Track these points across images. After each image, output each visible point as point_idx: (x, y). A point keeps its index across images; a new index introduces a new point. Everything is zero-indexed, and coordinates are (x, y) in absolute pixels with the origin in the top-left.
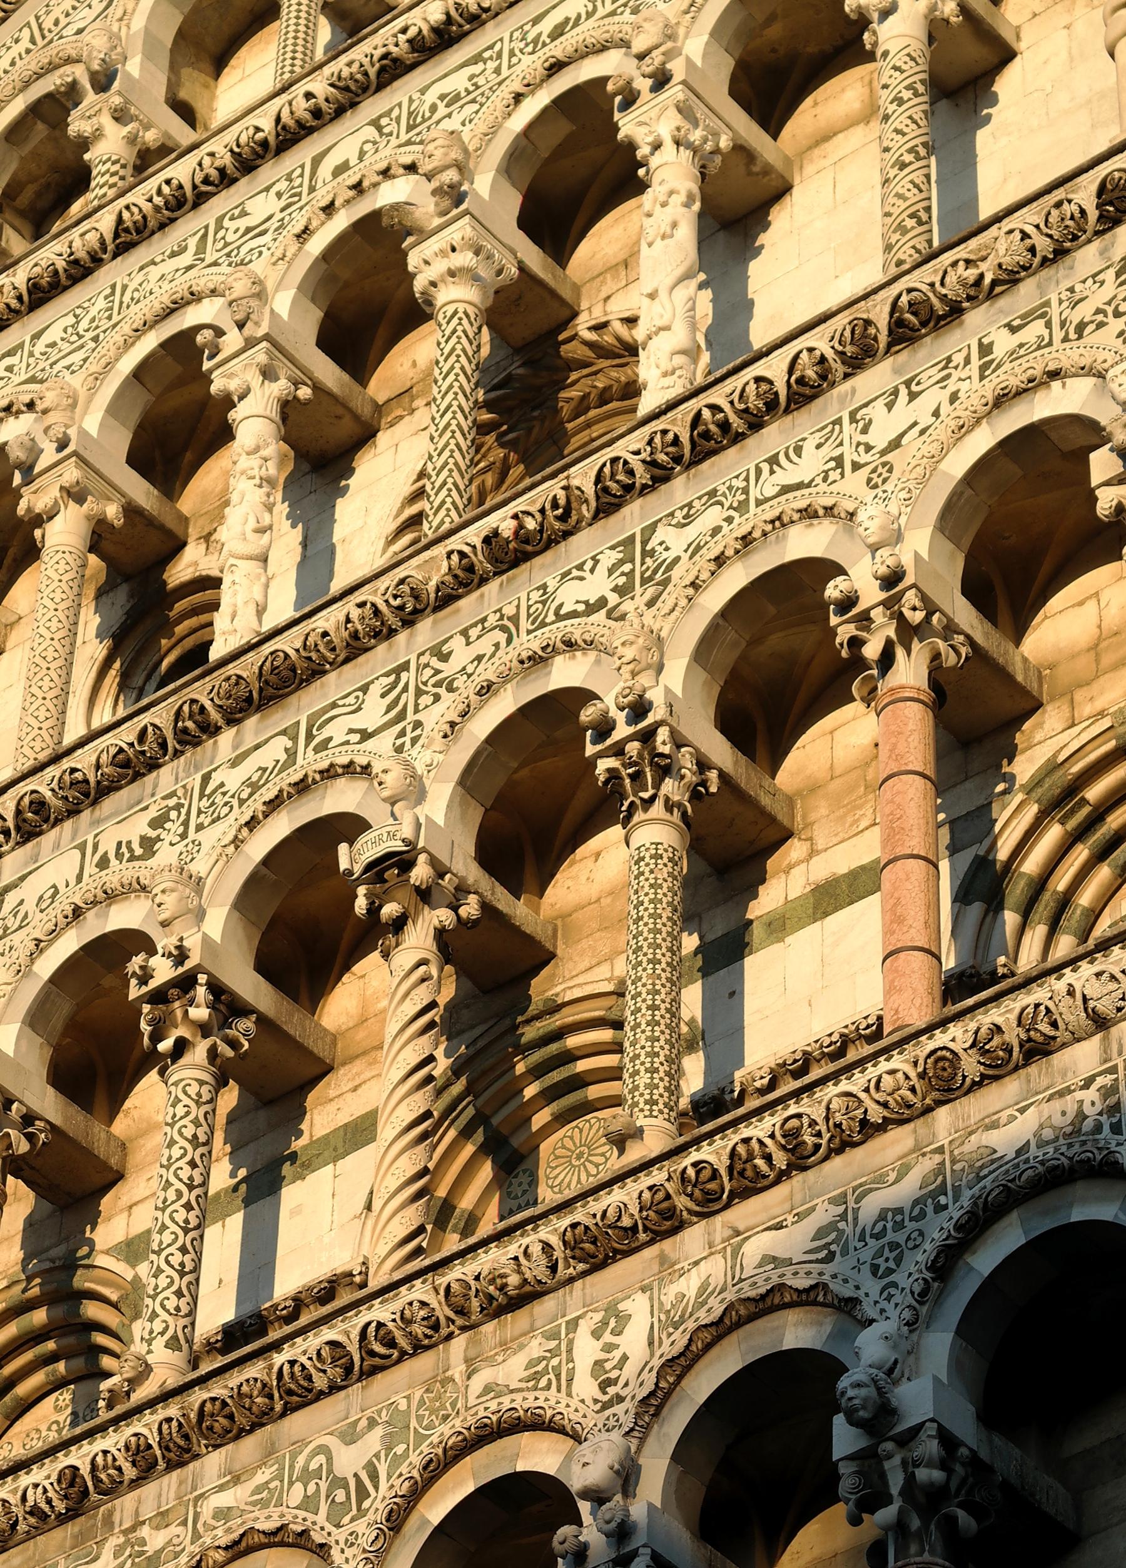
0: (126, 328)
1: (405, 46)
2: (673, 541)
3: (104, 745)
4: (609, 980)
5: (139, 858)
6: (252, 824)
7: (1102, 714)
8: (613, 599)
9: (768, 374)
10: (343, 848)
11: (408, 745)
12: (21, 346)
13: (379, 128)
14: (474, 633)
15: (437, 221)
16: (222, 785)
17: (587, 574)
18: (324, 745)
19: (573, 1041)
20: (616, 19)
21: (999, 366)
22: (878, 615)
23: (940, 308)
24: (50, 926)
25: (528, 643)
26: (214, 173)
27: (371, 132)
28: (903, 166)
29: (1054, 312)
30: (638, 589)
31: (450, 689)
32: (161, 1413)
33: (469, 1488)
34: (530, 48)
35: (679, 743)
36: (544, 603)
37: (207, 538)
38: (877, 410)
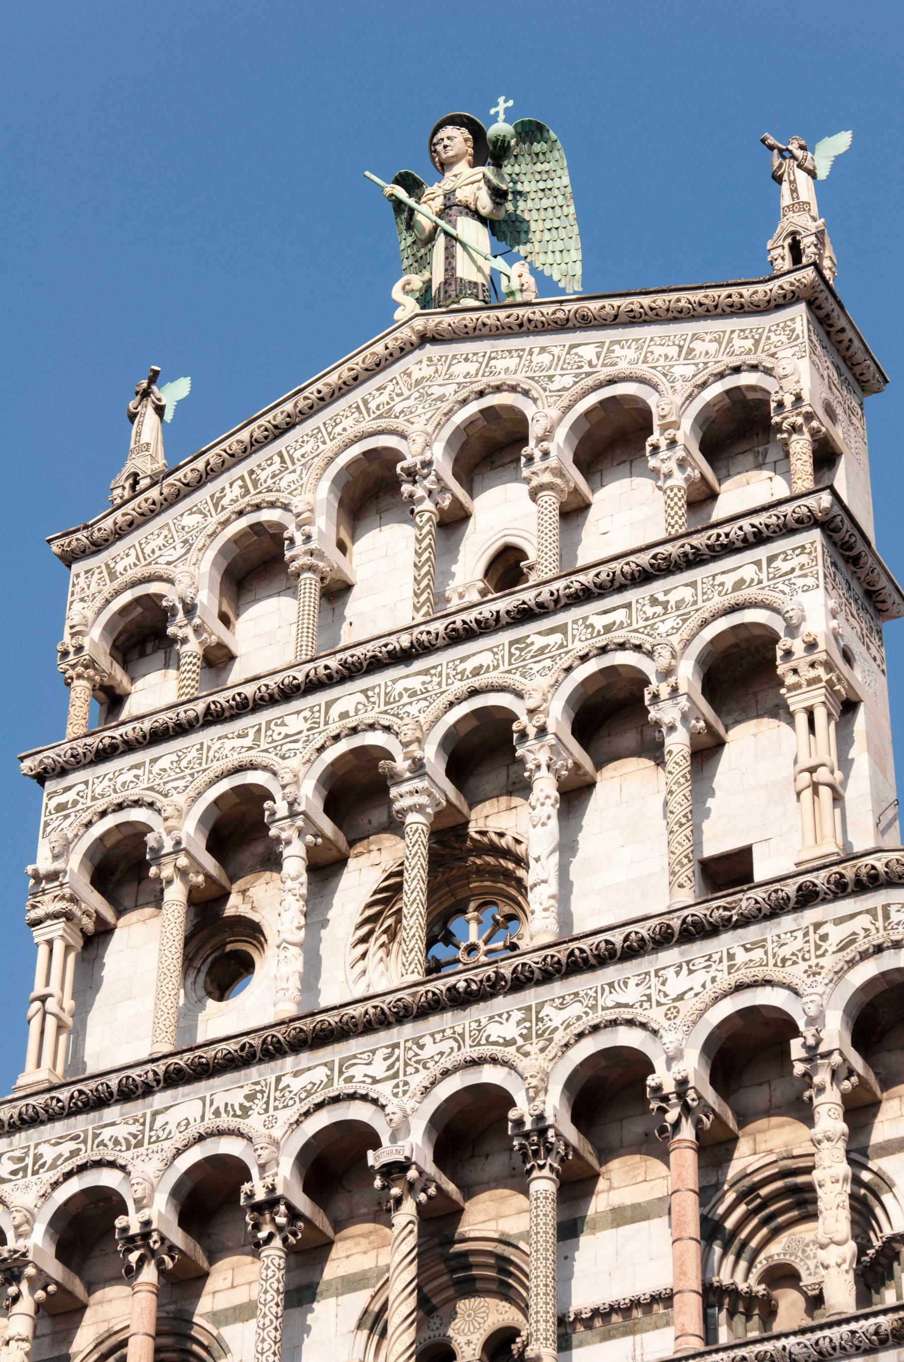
0: (211, 774)
1: (386, 656)
2: (555, 1017)
5: (239, 1116)
6: (307, 1114)
7: (771, 1151)
8: (520, 1041)
9: (613, 939)
10: (370, 1153)
11: (401, 1094)
12: (143, 764)
13: (367, 697)
14: (438, 1037)
15: (408, 775)
16: (288, 1086)
17: (504, 1021)
18: (350, 1079)
20: (512, 676)
21: (738, 969)
22: (673, 1099)
23: (708, 927)
24: (185, 1142)
25: (469, 1052)
27: (361, 698)
28: (681, 825)
29: (769, 946)
30: (534, 1040)
31: (425, 1068)
34: (459, 677)
35: (558, 1135)
36: (479, 1031)
37: (244, 892)
38: (670, 973)
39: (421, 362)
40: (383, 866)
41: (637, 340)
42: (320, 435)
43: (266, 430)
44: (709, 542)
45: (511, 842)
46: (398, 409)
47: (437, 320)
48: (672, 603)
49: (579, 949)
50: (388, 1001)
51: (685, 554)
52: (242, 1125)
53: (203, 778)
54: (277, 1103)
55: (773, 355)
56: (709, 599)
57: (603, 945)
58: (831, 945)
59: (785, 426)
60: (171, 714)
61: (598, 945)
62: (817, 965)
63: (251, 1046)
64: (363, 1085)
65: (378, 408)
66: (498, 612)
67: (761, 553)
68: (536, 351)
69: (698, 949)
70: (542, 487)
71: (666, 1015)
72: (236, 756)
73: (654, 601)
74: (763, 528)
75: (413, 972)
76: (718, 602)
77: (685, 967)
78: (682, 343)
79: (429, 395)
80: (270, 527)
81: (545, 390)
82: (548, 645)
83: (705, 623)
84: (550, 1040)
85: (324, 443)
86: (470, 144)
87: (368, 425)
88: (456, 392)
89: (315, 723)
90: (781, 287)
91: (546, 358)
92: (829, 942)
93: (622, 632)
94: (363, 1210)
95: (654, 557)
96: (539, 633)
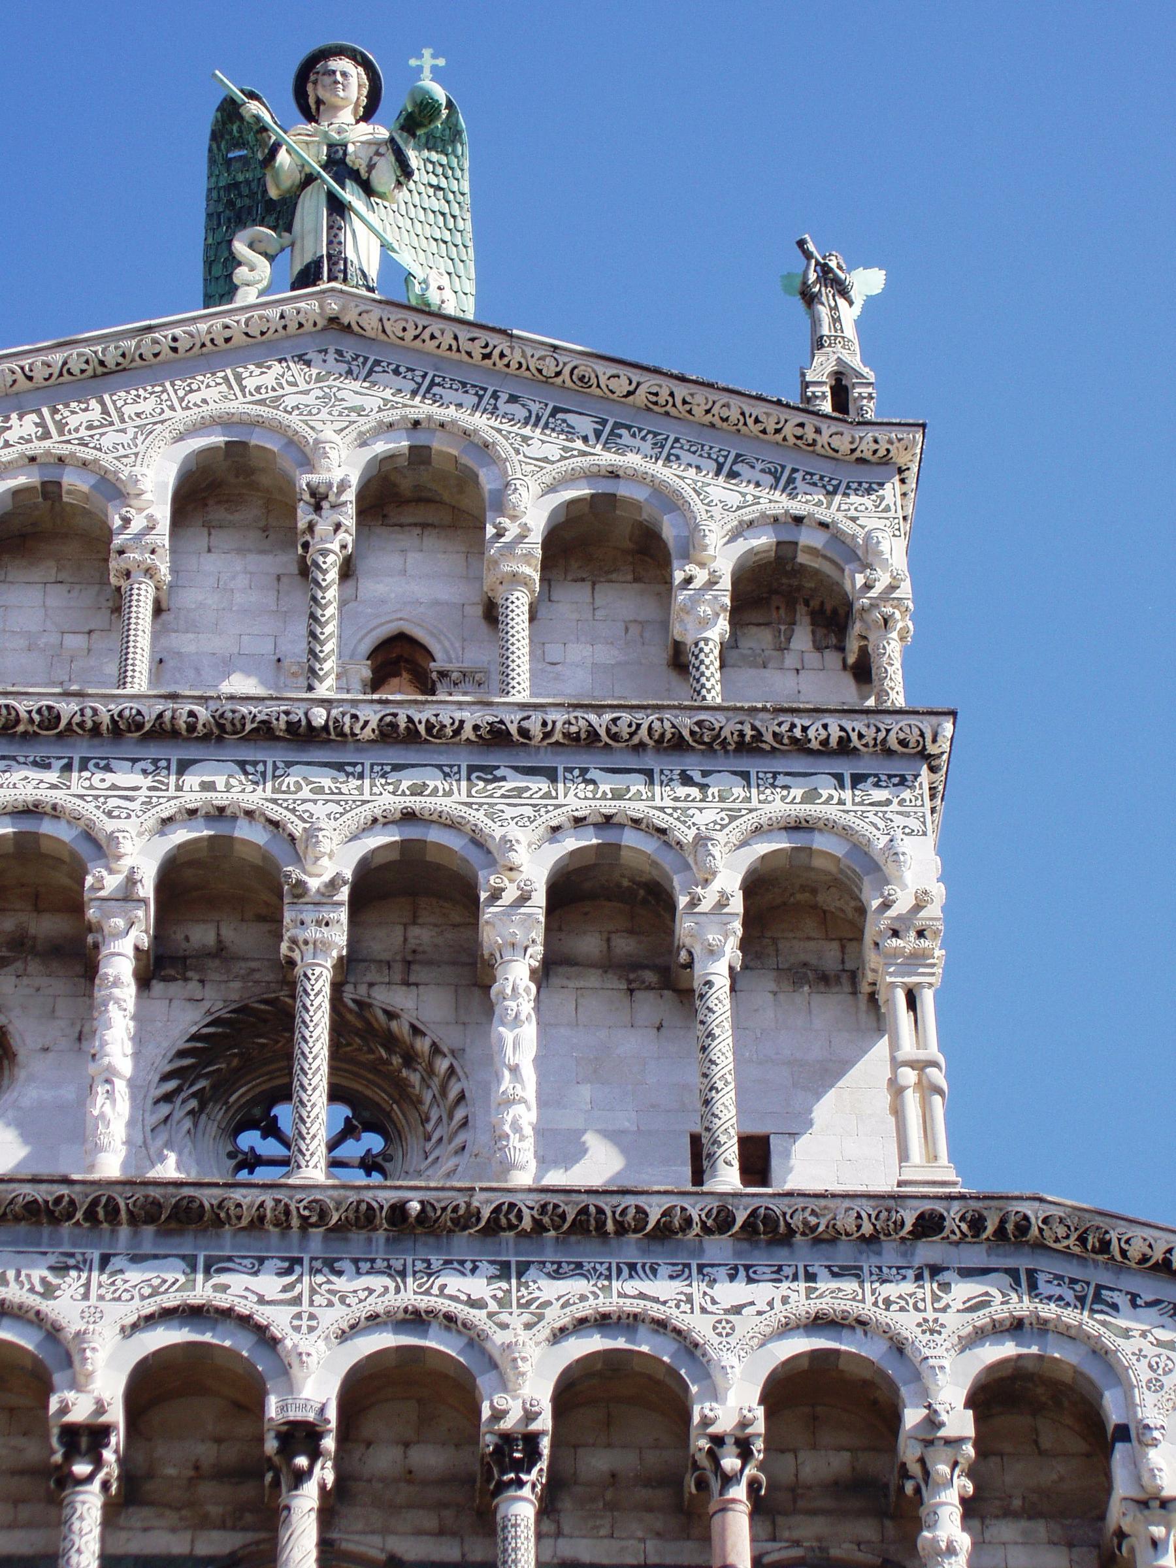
1: (283, 726)
3: (27, 1191)
4: (382, 1550)
7: (797, 1543)
8: (493, 1306)
11: (304, 1329)
17: (468, 1272)
20: (474, 813)
21: (820, 1296)
26: (89, 724)
31: (342, 1300)
39: (326, 351)
40: (207, 1005)
41: (656, 434)
42: (165, 396)
43: (87, 362)
44: (777, 729)
45: (406, 1029)
46: (290, 401)
47: (362, 308)
49: (596, 1206)
50: (298, 1197)
51: (742, 734)
54: (102, 1291)
55: (854, 519)
56: (765, 801)
57: (632, 1211)
61: (626, 1208)
62: (936, 1320)
63: (72, 1202)
64: (244, 1302)
65: (258, 389)
66: (462, 722)
67: (847, 769)
68: (504, 397)
71: (715, 1328)
72: (30, 789)
74: (854, 736)
75: (316, 1167)
77: (741, 1269)
78: (721, 460)
79: (337, 399)
80: (69, 492)
81: (517, 452)
82: (528, 789)
84: (541, 1317)
85: (172, 408)
86: (365, 92)
88: (380, 410)
89: (162, 783)
90: (876, 441)
92: (952, 1295)
93: (640, 805)
94: (171, 1471)
95: (699, 723)
96: (516, 769)
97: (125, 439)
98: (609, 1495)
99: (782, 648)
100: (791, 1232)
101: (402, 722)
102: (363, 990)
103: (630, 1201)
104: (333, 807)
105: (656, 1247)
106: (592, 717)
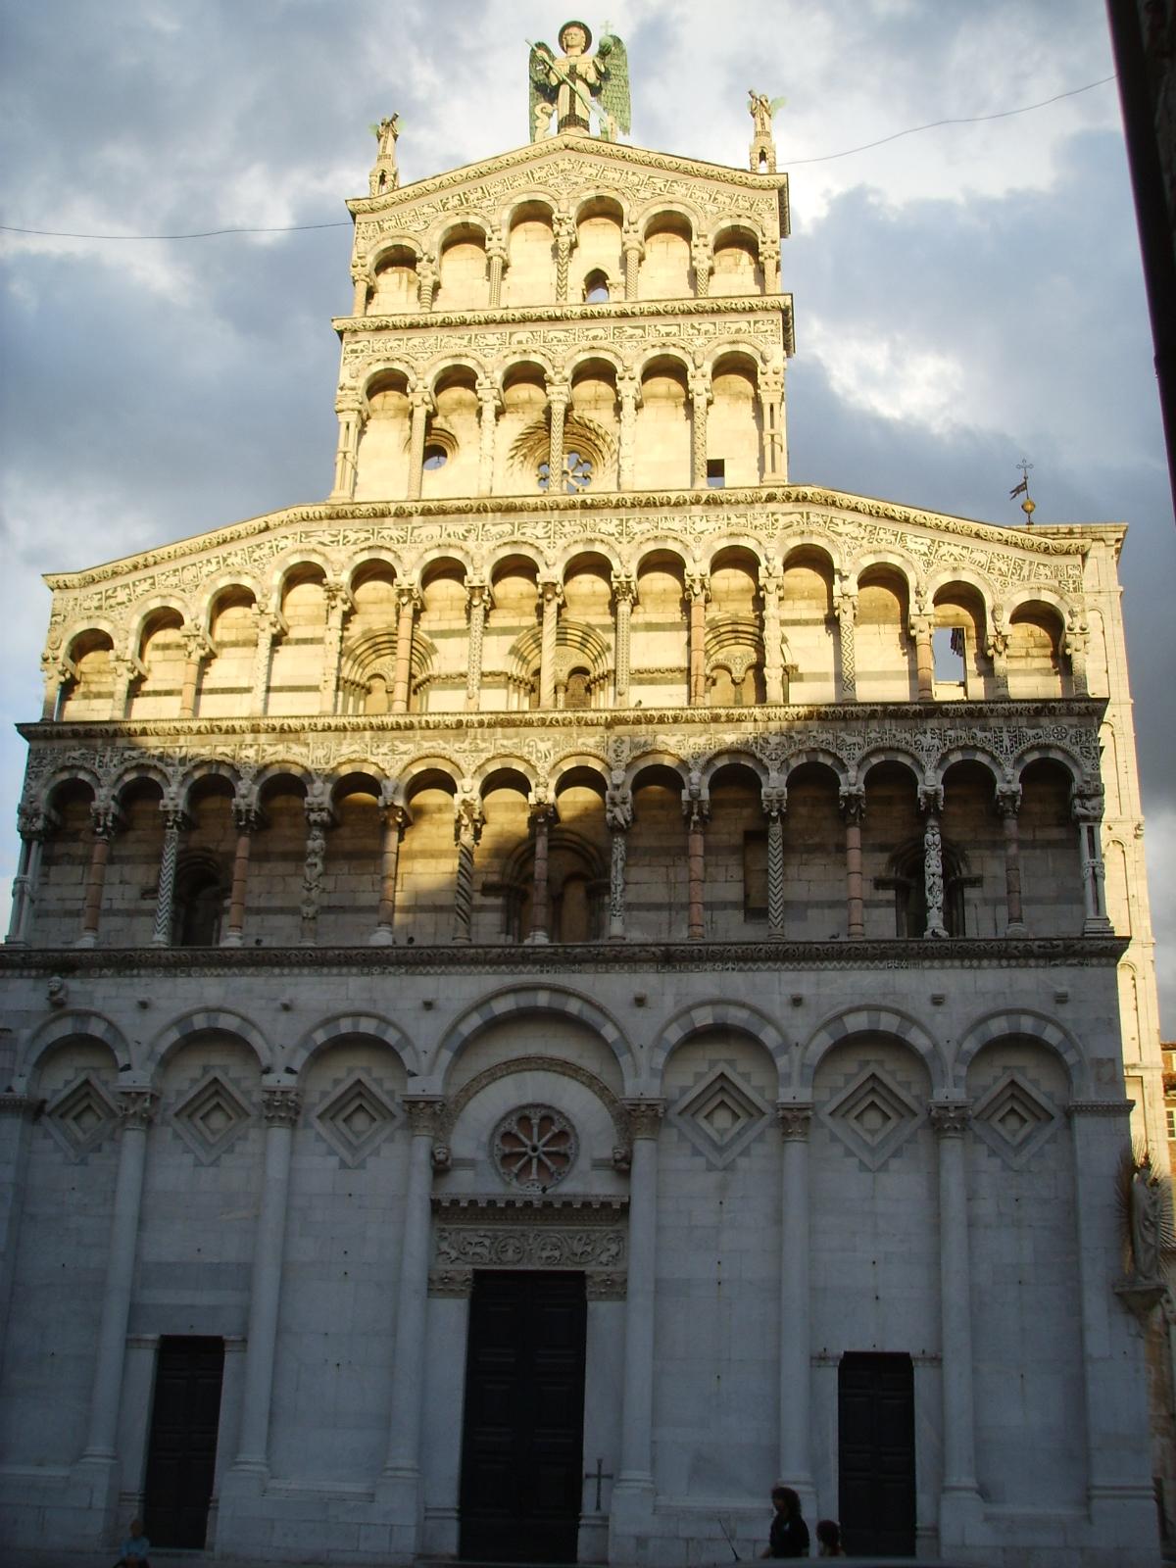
7: (727, 612)
8: (617, 535)
19: (569, 631)
22: (697, 581)
32: (490, 716)
33: (575, 765)
38: (697, 519)
46: (551, 182)
48: (702, 331)
52: (464, 545)
53: (439, 356)
58: (780, 525)
59: (766, 254)
60: (423, 317)
67: (751, 317)
69: (713, 512)
70: (633, 248)
73: (693, 327)
76: (727, 337)
83: (719, 345)
87: (533, 186)
91: (636, 179)
97: (490, 203)
98: (663, 597)
99: (737, 265)
100: (722, 503)
101: (589, 313)
102: (580, 413)
103: (665, 494)
104: (565, 347)
105: (675, 509)
106: (657, 305)
